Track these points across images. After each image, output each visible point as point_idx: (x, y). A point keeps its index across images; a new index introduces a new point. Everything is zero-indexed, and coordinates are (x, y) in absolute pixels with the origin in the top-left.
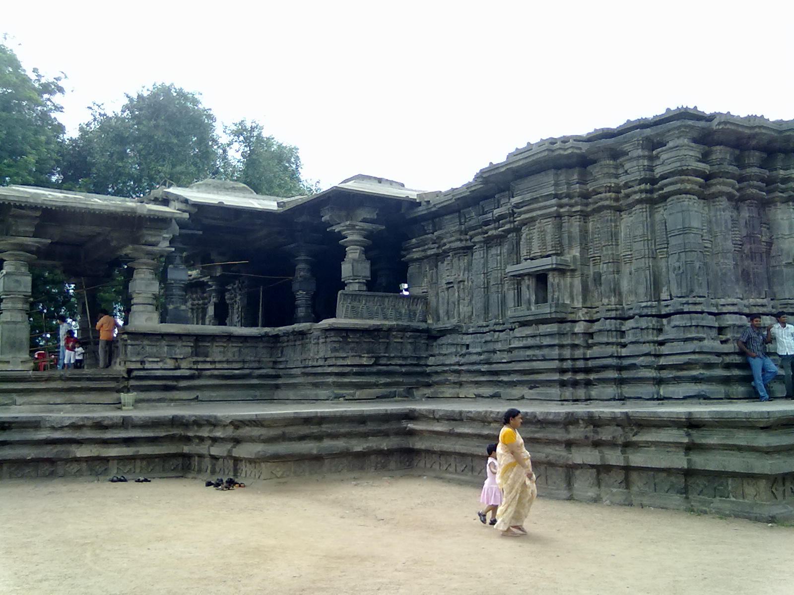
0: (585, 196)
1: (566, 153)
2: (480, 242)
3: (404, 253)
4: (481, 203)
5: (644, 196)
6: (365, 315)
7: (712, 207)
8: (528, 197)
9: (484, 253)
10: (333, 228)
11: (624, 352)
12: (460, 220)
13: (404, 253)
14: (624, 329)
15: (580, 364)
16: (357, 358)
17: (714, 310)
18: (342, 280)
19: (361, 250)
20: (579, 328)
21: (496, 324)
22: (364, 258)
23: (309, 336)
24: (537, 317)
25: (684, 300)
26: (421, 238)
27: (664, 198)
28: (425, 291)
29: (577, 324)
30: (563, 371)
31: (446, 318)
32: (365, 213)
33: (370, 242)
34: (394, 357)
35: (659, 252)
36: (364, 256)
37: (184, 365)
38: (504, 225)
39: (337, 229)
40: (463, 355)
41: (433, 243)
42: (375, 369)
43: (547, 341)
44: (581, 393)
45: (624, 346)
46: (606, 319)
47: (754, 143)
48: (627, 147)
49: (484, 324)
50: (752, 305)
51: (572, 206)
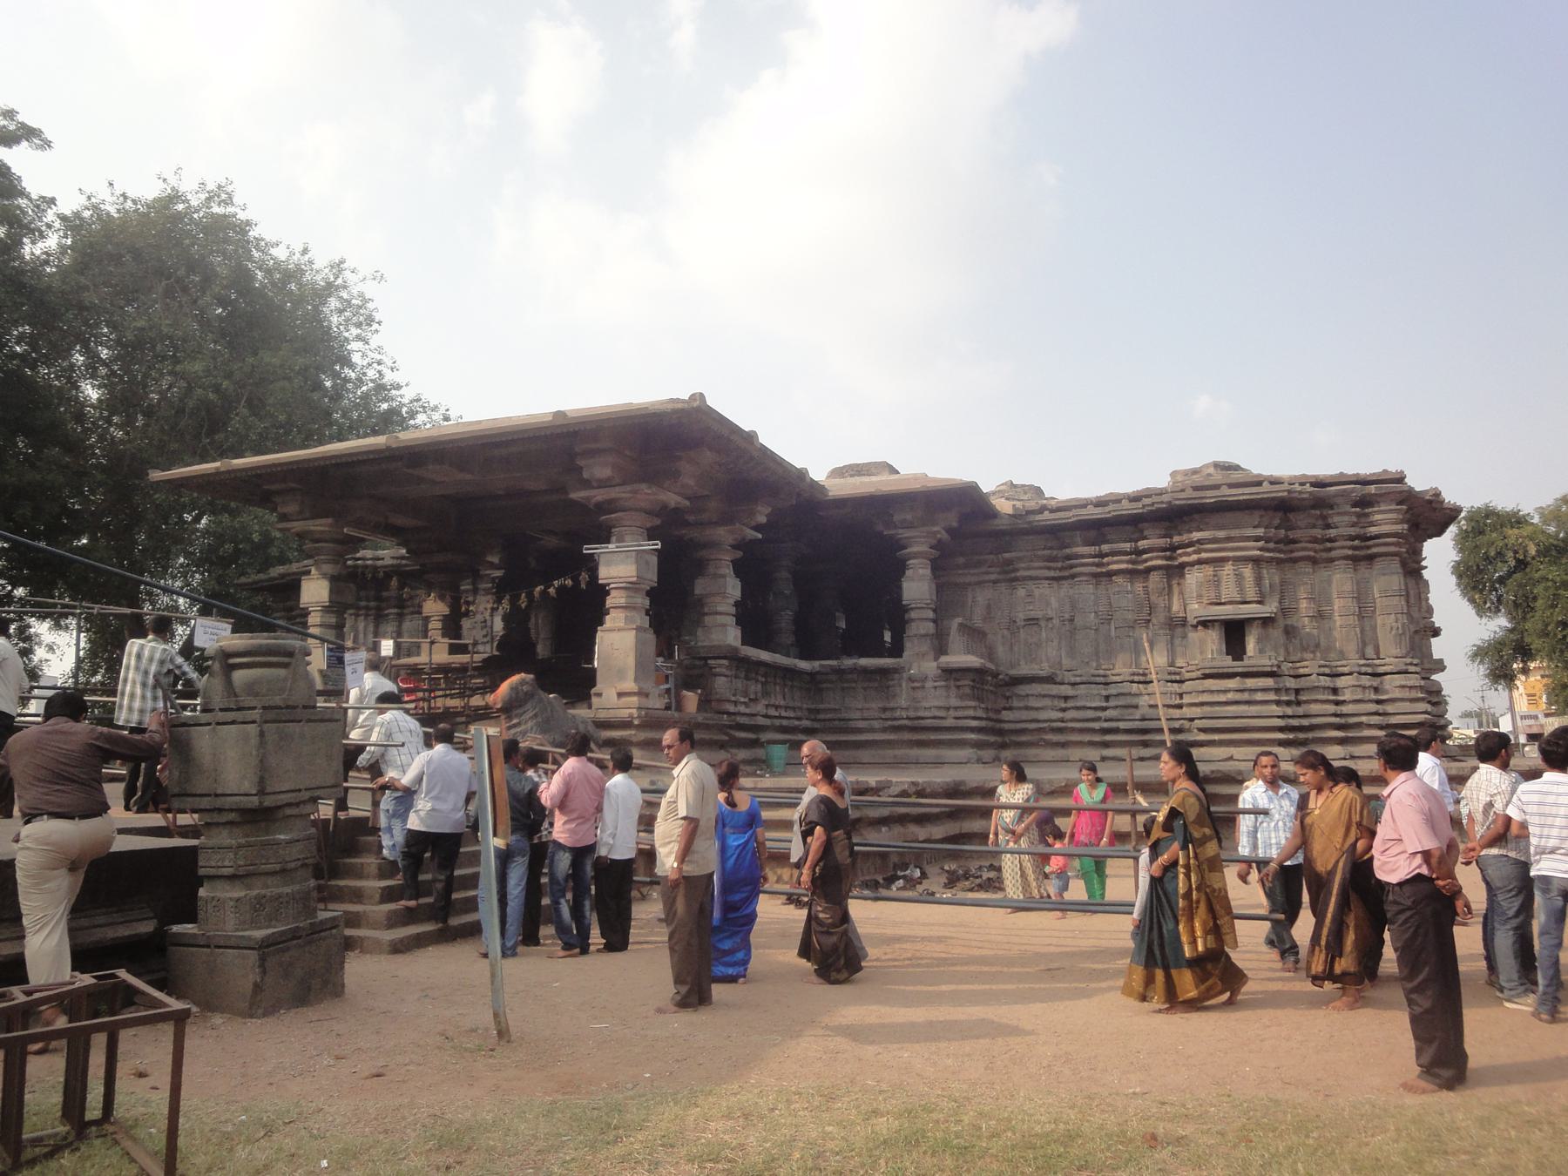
5: (1350, 552)
8: (1221, 534)
27: (1371, 558)
37: (760, 708)
38: (1151, 559)
39: (906, 533)
40: (1064, 710)
43: (1259, 696)
48: (1339, 500)
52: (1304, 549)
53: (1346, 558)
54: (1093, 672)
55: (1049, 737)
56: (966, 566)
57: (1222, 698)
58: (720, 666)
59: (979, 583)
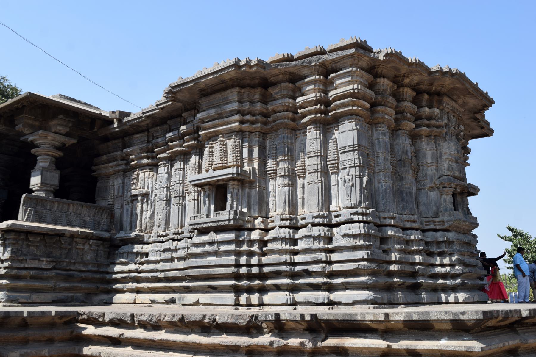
0: (266, 115)
1: (251, 70)
3: (94, 168)
4: (169, 122)
6: (49, 219)
7: (374, 131)
9: (168, 168)
10: (26, 137)
11: (297, 259)
12: (148, 138)
13: (94, 168)
14: (296, 237)
15: (255, 270)
16: (36, 262)
17: (378, 221)
18: (31, 187)
19: (51, 161)
20: (255, 235)
21: (175, 234)
22: (54, 168)
24: (217, 224)
25: (354, 210)
26: (111, 154)
28: (112, 203)
29: (253, 232)
30: (237, 277)
31: (128, 228)
32: (58, 125)
33: (61, 154)
34: (74, 263)
35: (330, 167)
36: (54, 167)
39: (31, 138)
40: (142, 263)
41: (121, 160)
42: (53, 273)
43: (224, 248)
44: (255, 298)
45: (296, 253)
46: (281, 227)
47: (407, 81)
48: (305, 72)
49: (164, 234)
50: (405, 221)
51: (253, 123)
53: (313, 122)
54: (161, 233)
56: (109, 161)
57: (199, 250)
59: (115, 173)
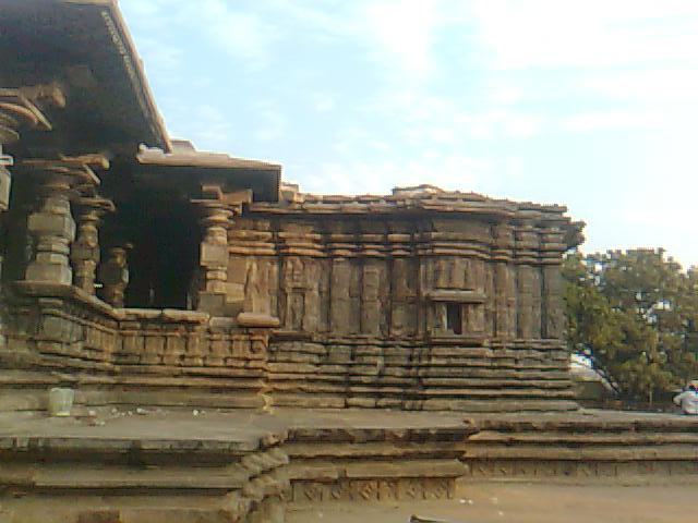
2: (345, 257)
8: (452, 235)
11: (521, 374)
23: (197, 328)
39: (211, 203)
45: (518, 370)
52: (503, 254)
55: (305, 386)
58: (54, 306)
